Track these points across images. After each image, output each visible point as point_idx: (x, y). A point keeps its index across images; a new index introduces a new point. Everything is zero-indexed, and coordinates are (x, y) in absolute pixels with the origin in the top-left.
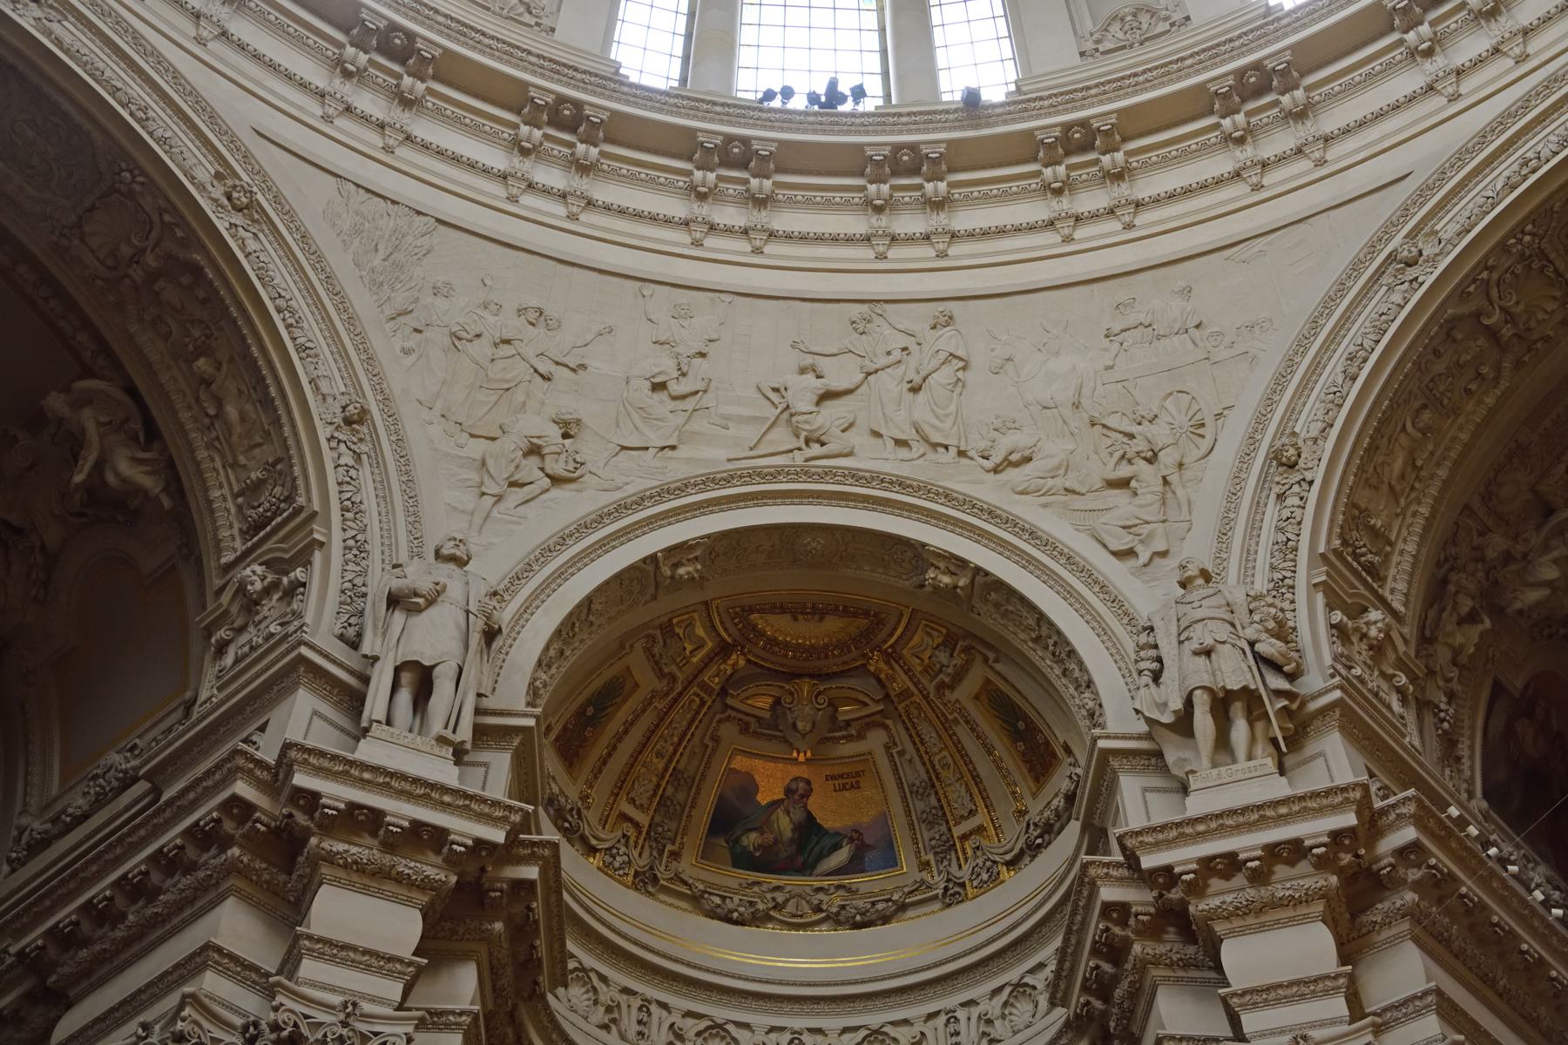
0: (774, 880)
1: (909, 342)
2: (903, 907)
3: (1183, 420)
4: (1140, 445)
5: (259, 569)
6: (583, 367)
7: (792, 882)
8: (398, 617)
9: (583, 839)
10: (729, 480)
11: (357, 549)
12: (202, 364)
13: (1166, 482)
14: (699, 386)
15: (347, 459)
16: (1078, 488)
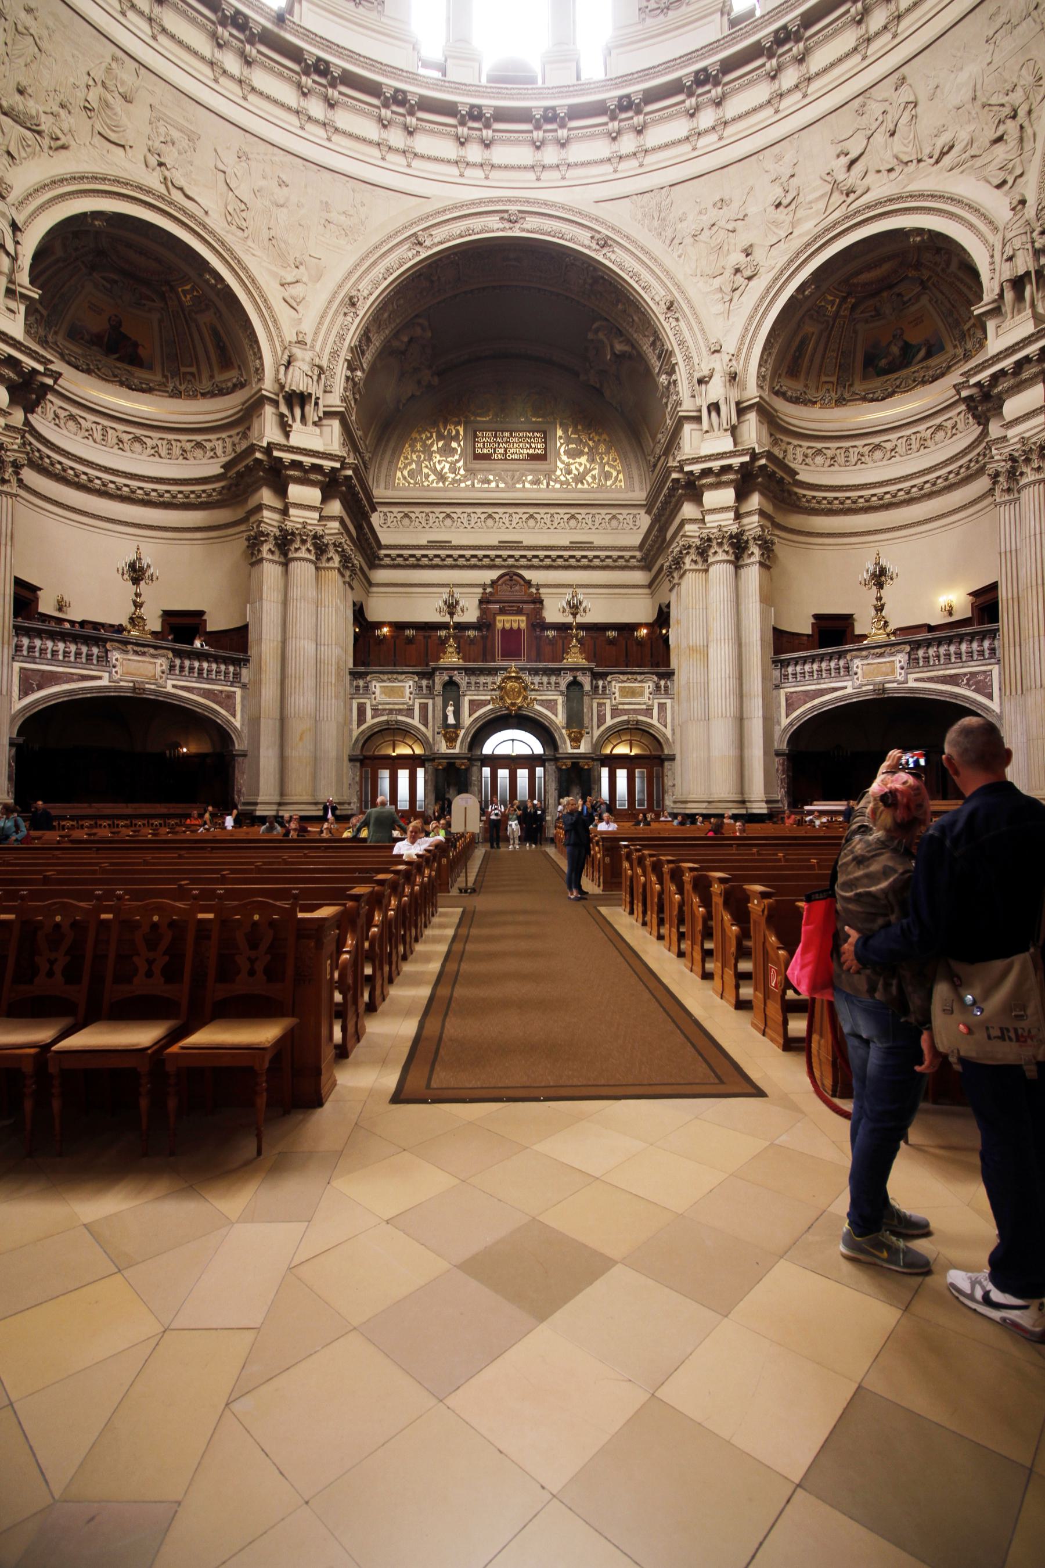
0: (895, 376)
1: (885, 106)
2: (949, 367)
3: (1030, 79)
4: (1007, 111)
5: (664, 376)
6: (745, 215)
7: (904, 373)
8: (704, 386)
9: (810, 401)
10: (815, 240)
11: (688, 358)
12: (620, 306)
13: (1022, 127)
14: (795, 194)
15: (674, 323)
16: (978, 154)
